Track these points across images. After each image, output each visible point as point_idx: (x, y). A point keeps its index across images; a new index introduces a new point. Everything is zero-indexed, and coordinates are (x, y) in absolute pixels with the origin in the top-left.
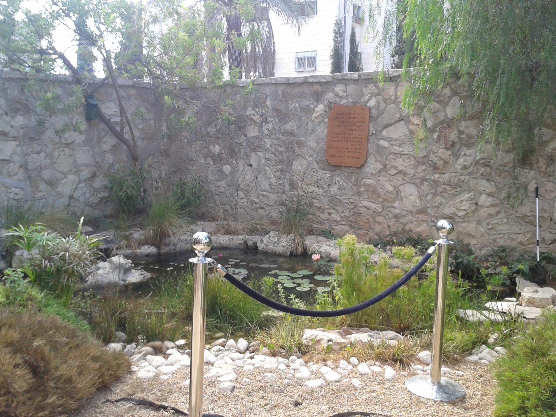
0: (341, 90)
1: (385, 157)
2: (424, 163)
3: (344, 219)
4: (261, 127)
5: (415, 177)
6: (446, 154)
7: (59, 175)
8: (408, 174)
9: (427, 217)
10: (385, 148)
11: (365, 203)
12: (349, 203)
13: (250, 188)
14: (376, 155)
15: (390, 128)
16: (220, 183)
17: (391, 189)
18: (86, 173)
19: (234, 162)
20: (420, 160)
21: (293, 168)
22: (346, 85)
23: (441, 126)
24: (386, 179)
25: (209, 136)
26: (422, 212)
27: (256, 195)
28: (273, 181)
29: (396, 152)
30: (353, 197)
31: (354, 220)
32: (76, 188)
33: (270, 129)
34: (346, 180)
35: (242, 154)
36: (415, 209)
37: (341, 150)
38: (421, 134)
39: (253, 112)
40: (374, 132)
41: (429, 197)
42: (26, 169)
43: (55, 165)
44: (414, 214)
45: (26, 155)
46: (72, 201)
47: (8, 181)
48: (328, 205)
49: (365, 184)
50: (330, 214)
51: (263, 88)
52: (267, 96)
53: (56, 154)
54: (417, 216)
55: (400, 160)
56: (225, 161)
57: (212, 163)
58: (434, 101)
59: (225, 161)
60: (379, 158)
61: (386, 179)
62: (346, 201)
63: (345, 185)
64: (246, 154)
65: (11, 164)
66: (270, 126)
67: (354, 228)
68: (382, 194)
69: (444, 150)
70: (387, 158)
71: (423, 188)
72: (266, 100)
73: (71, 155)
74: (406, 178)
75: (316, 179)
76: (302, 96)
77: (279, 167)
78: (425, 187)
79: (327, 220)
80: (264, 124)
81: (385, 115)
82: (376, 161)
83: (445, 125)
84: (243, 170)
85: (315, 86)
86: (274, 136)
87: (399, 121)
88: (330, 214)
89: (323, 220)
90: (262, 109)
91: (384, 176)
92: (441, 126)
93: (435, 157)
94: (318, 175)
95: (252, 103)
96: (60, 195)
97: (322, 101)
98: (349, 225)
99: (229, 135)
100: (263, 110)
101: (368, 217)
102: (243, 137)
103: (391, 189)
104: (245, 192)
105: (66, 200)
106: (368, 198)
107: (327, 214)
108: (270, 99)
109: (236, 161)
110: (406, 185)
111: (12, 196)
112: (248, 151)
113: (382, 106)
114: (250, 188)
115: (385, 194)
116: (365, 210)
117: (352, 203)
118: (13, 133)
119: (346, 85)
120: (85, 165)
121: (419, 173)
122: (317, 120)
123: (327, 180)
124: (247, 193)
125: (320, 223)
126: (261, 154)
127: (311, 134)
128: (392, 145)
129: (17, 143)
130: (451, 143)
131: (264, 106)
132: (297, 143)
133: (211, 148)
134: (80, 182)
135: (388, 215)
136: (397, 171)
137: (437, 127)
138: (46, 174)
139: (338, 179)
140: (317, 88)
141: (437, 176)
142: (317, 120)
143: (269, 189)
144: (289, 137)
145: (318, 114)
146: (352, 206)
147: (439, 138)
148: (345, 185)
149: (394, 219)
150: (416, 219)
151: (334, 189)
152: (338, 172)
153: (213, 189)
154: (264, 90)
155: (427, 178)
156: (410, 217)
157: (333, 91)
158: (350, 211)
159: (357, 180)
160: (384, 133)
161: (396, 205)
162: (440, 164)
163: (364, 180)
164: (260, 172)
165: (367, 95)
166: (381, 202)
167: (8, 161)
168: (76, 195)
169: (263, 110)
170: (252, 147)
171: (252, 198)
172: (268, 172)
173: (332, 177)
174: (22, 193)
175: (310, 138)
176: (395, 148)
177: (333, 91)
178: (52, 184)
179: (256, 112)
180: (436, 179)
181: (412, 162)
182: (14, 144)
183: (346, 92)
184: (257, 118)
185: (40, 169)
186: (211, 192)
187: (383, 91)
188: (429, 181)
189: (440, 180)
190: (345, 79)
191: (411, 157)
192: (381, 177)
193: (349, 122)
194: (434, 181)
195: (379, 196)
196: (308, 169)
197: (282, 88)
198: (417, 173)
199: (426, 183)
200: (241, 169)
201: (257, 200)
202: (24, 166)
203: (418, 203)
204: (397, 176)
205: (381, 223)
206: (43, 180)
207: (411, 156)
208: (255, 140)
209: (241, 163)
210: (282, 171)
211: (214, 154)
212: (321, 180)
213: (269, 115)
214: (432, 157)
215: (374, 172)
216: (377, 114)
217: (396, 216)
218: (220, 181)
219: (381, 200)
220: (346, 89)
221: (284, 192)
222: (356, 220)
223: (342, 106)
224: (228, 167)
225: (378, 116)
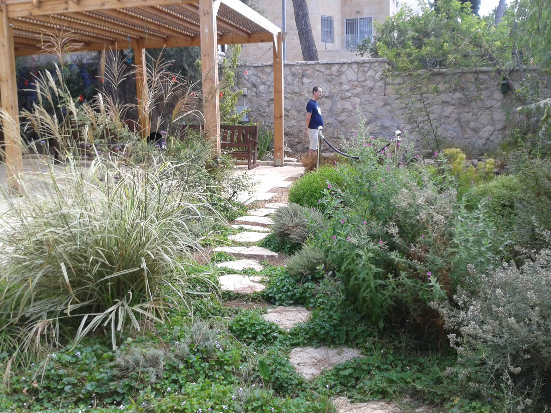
7: (480, 126)
18: (499, 126)
32: (492, 135)
42: (459, 121)
43: (479, 120)
45: (460, 114)
46: (488, 141)
47: (448, 127)
53: (479, 113)
65: (450, 119)
73: (490, 115)
96: (480, 138)
105: (484, 141)
111: (449, 135)
118: (453, 102)
120: (499, 121)
129: (454, 107)
134: (495, 131)
138: (472, 125)
167: (448, 117)
168: (491, 138)
174: (456, 134)
178: (475, 130)
182: (452, 108)
185: (468, 122)
202: (458, 120)
206: (470, 128)
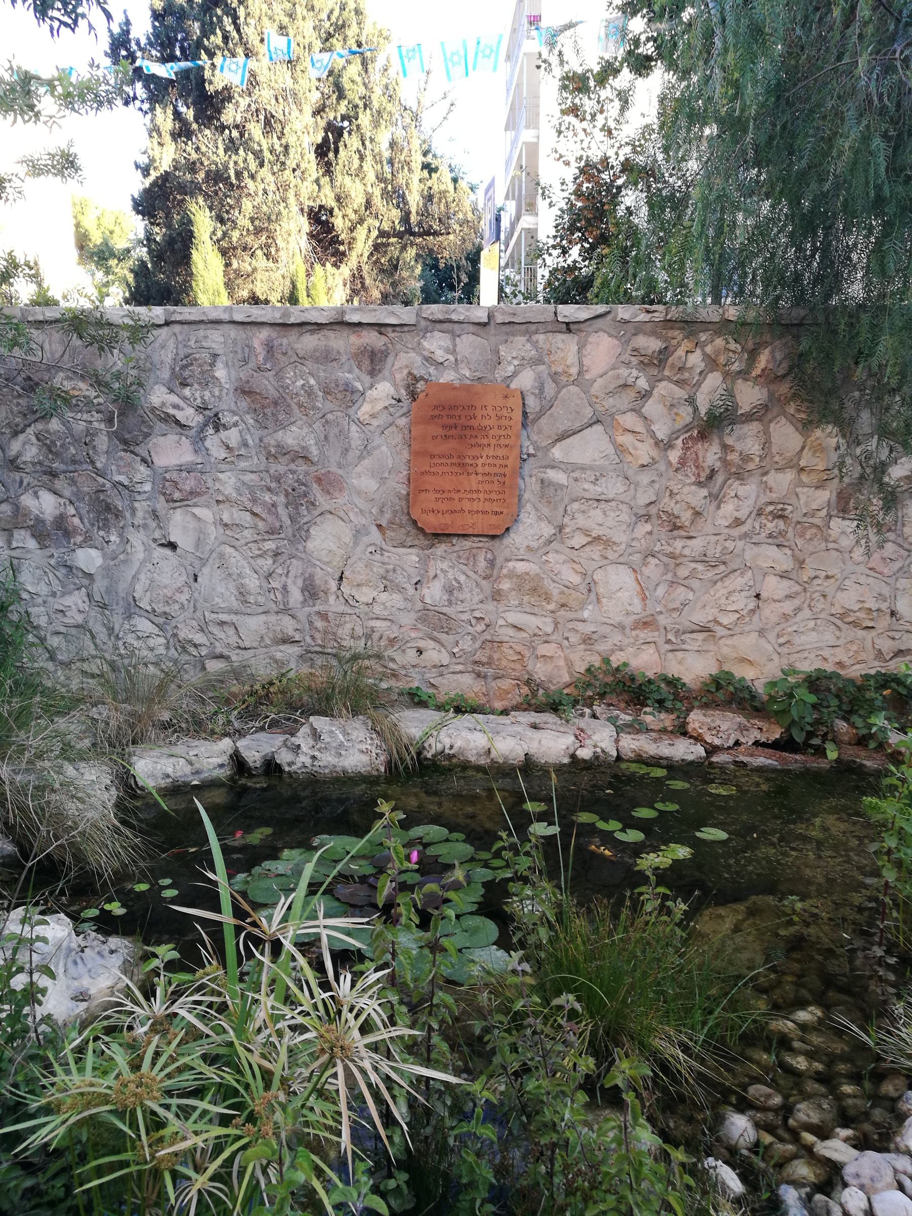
0: (440, 347)
1: (562, 510)
2: (648, 518)
3: (461, 660)
4: (199, 440)
5: (630, 550)
6: (697, 496)
8: (615, 543)
9: (656, 634)
10: (562, 486)
11: (513, 617)
12: (473, 621)
13: (177, 607)
14: (540, 506)
15: (568, 441)
16: (68, 601)
17: (576, 579)
19: (113, 538)
20: (642, 512)
21: (310, 545)
22: (454, 336)
23: (687, 435)
24: (563, 557)
25: (18, 469)
26: (645, 623)
27: (194, 623)
28: (252, 582)
29: (587, 495)
30: (480, 605)
31: (485, 660)
33: (233, 443)
34: (464, 567)
35: (140, 514)
36: (628, 621)
37: (453, 495)
38: (644, 451)
39: (174, 399)
40: (531, 451)
41: (660, 591)
44: (627, 631)
48: (415, 628)
49: (511, 575)
50: (420, 652)
51: (201, 333)
52: (215, 356)
54: (634, 633)
55: (597, 514)
56: (79, 539)
57: (32, 544)
58: (669, 379)
59: (79, 539)
60: (546, 511)
61: (563, 557)
62: (465, 617)
63: (462, 578)
64: (155, 515)
66: (232, 436)
67: (485, 677)
68: (555, 592)
69: (693, 488)
70: (565, 511)
71: (646, 571)
72: (212, 365)
74: (612, 555)
75: (382, 571)
76: (327, 357)
77: (270, 545)
78: (653, 569)
79: (414, 666)
80: (211, 431)
81: (557, 410)
82: (539, 518)
83: (695, 434)
84: (147, 560)
85: (364, 333)
86: (243, 464)
87: (591, 425)
88: (420, 652)
89: (403, 667)
90: (203, 389)
91: (557, 552)
92: (687, 435)
93: (677, 502)
94: (386, 560)
95: (166, 374)
97: (386, 373)
98: (473, 671)
99: (92, 462)
100: (207, 394)
101: (519, 648)
102: (142, 468)
103: (576, 579)
104: (161, 620)
106: (520, 605)
107: (412, 653)
108: (227, 365)
109: (121, 536)
110: (609, 568)
112: (161, 505)
113: (550, 389)
114: (177, 607)
115: (562, 593)
116: (511, 632)
117: (479, 619)
119: (454, 336)
121: (639, 540)
122: (375, 423)
123: (411, 570)
124: (163, 620)
125: (395, 675)
126: (204, 513)
127: (361, 458)
128: (576, 480)
130: (708, 472)
131: (208, 380)
132: (319, 480)
133: (27, 500)
135: (567, 639)
136: (590, 539)
137: (677, 438)
139: (445, 566)
140: (371, 338)
141: (679, 544)
142: (375, 423)
143: (235, 604)
144: (293, 466)
145: (380, 406)
146: (480, 627)
147: (683, 462)
148: (462, 578)
149: (583, 646)
150: (632, 640)
151: (434, 593)
152: (441, 549)
153: (43, 621)
154: (206, 337)
155: (656, 549)
156: (616, 638)
157: (418, 348)
158: (474, 639)
159: (492, 563)
160: (557, 452)
161: (586, 614)
162: (686, 517)
163: (511, 564)
164: (204, 562)
165: (510, 363)
166: (552, 612)
169: (207, 394)
170: (177, 495)
171: (184, 633)
172: (233, 560)
173: (424, 562)
175: (359, 469)
176: (586, 486)
177: (418, 348)
179: (184, 399)
180: (678, 552)
181: (625, 517)
183: (453, 352)
184: (189, 415)
186: (37, 628)
187: (550, 353)
188: (659, 556)
189: (687, 552)
190: (451, 321)
191: (621, 506)
192: (550, 555)
193: (471, 428)
194: (672, 556)
195: (548, 598)
196: (356, 544)
197: (265, 333)
198: (633, 539)
199: (653, 561)
200: (141, 556)
201: (199, 638)
203: (637, 606)
204: (588, 549)
205: (551, 658)
207: (622, 502)
208: (184, 474)
209: (137, 539)
210: (276, 554)
211: (39, 521)
212: (394, 570)
213: (225, 407)
214: (668, 504)
215: (535, 544)
216: (538, 409)
217: (588, 640)
218: (64, 594)
219: (552, 607)
220: (455, 345)
221: (286, 610)
222: (490, 657)
223: (449, 386)
224: (93, 552)
225: (541, 413)
